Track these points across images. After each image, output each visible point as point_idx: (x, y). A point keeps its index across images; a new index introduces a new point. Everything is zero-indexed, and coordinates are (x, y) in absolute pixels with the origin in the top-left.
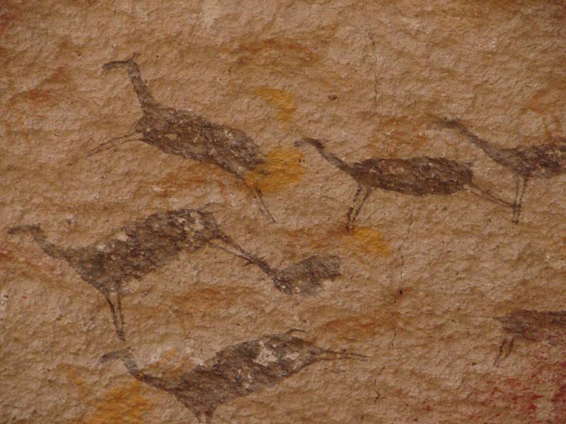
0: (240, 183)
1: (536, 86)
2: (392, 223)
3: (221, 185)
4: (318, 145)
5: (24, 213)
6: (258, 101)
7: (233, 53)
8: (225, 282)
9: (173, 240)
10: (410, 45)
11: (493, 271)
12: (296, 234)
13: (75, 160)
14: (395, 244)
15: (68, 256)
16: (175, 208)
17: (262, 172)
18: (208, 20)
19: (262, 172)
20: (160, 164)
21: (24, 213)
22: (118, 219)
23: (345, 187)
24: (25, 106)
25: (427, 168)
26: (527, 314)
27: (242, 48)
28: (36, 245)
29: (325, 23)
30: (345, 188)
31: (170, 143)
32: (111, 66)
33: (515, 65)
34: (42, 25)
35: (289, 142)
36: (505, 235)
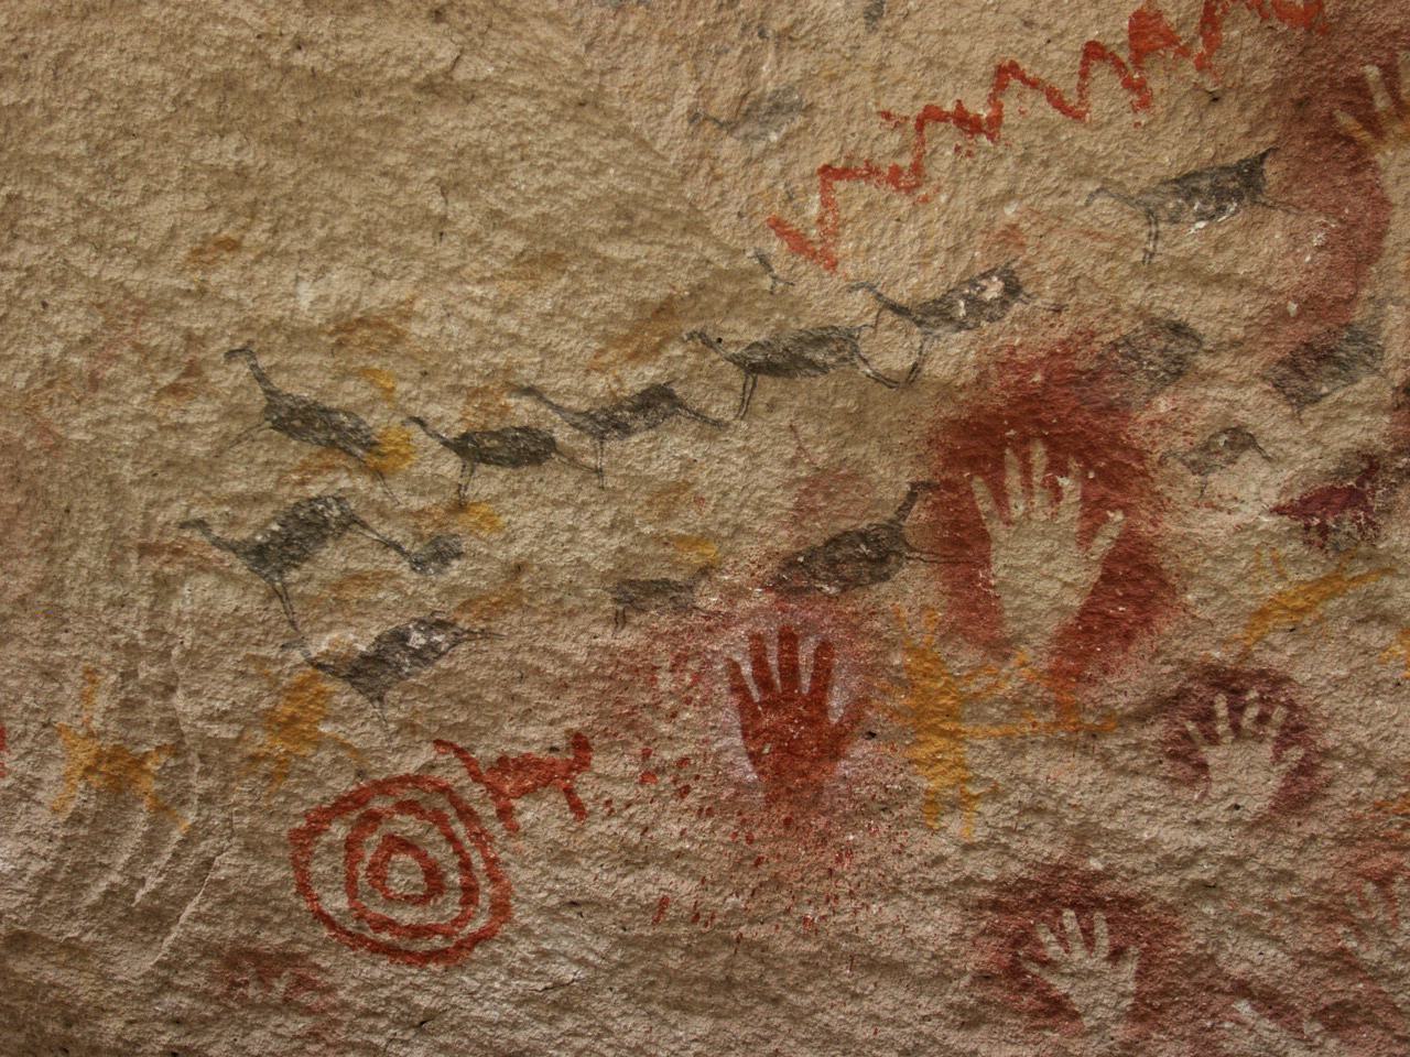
0: (364, 469)
1: (595, 345)
2: (497, 498)
3: (348, 470)
4: (421, 422)
5: (190, 507)
6: (362, 383)
7: (331, 334)
8: (371, 567)
9: (319, 527)
10: (479, 313)
11: (593, 540)
12: (420, 513)
13: (220, 452)
14: (505, 519)
15: (232, 547)
16: (313, 495)
17: (379, 454)
18: (304, 304)
19: (379, 454)
20: (295, 453)
21: (190, 507)
22: (268, 510)
23: (451, 463)
24: (169, 401)
25: (516, 439)
26: (632, 583)
27: (338, 330)
28: (205, 539)
29: (403, 298)
30: (450, 466)
31: (296, 430)
32: (231, 355)
33: (573, 326)
34: (168, 319)
35: (397, 420)
36: (596, 502)
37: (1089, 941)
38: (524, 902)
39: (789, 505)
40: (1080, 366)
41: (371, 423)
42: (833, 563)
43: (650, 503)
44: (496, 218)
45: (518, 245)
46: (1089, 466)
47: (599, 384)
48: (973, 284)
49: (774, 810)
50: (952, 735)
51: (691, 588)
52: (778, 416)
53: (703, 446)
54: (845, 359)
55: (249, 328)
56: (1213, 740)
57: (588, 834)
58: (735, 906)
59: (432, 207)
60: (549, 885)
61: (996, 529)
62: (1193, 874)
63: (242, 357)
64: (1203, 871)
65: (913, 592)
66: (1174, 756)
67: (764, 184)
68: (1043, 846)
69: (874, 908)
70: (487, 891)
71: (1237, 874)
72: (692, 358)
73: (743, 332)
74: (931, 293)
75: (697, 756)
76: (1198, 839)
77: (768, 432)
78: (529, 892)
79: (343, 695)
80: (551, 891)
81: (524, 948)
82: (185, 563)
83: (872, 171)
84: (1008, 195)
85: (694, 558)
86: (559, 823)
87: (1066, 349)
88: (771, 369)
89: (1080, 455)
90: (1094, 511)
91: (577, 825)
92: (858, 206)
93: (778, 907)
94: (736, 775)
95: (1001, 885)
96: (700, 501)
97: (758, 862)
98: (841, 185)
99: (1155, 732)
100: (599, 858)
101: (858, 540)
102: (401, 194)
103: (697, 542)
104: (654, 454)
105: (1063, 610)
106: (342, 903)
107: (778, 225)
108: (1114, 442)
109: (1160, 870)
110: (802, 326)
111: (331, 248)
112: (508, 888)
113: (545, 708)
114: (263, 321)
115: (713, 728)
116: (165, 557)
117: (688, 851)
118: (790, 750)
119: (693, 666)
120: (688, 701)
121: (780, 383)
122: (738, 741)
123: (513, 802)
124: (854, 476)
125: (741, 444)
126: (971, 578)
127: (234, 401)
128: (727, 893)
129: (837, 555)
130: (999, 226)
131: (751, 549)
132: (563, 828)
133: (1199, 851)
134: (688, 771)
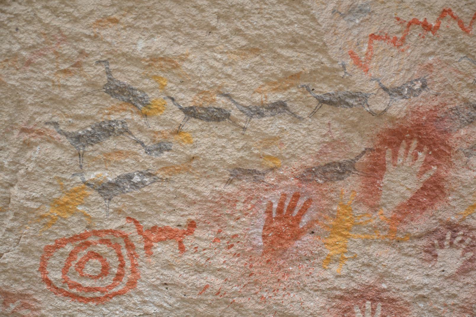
1: (261, 83)
2: (195, 132)
3: (132, 112)
4: (173, 99)
8: (126, 149)
9: (109, 131)
10: (216, 64)
11: (231, 152)
14: (196, 139)
15: (66, 135)
16: (112, 119)
17: (149, 108)
18: (139, 48)
22: (88, 122)
23: (180, 116)
26: (239, 169)
28: (55, 130)
29: (184, 53)
30: (180, 117)
33: (255, 75)
35: (162, 97)
38: (144, 281)
39: (317, 150)
41: (150, 96)
43: (261, 142)
44: (237, 31)
45: (244, 43)
47: (258, 98)
49: (264, 257)
51: (264, 174)
52: (325, 119)
53: (291, 125)
54: (361, 104)
55: (111, 54)
57: (183, 259)
58: (236, 290)
59: (211, 22)
60: (158, 276)
63: (103, 64)
70: (128, 276)
72: (299, 94)
73: (325, 89)
75: (242, 234)
77: (318, 124)
78: (148, 278)
79: (94, 196)
80: (158, 279)
81: (137, 299)
82: (42, 138)
85: (271, 164)
86: (172, 253)
88: (330, 103)
91: (179, 255)
93: (253, 292)
94: (255, 243)
96: (282, 144)
97: (251, 274)
100: (184, 268)
101: (337, 165)
102: (199, 15)
103: (274, 159)
104: (271, 125)
106: (59, 276)
110: (349, 90)
111: (159, 29)
112: (139, 276)
113: (182, 210)
114: (119, 52)
115: (252, 225)
116: (33, 134)
117: (225, 269)
118: (280, 235)
119: (253, 202)
120: (246, 214)
122: (261, 231)
123: (153, 244)
125: (306, 126)
127: (93, 80)
128: (234, 285)
129: (328, 169)
131: (296, 164)
132: (172, 256)
134: (236, 239)
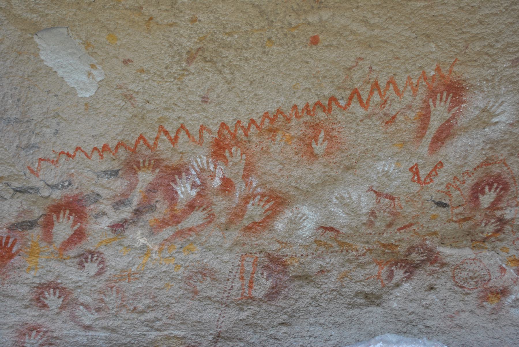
37: (55, 294)
40: (79, 198)
42: (22, 226)
46: (76, 215)
48: (63, 182)
50: (37, 257)
56: (87, 262)
61: (56, 223)
62: (78, 285)
64: (79, 284)
65: (37, 232)
66: (79, 264)
67: (28, 160)
68: (50, 278)
69: (12, 286)
71: (86, 285)
72: (4, 187)
73: (16, 184)
74: (55, 183)
76: (80, 279)
83: (49, 160)
84: (73, 168)
87: (77, 195)
88: (20, 192)
89: (75, 213)
90: (75, 222)
92: (45, 166)
95: (40, 284)
98: (42, 162)
99: (77, 260)
105: (65, 238)
107: (29, 168)
108: (82, 212)
109: (72, 283)
121: (21, 194)
124: (31, 211)
126: (49, 231)
130: (70, 173)
133: (80, 281)
